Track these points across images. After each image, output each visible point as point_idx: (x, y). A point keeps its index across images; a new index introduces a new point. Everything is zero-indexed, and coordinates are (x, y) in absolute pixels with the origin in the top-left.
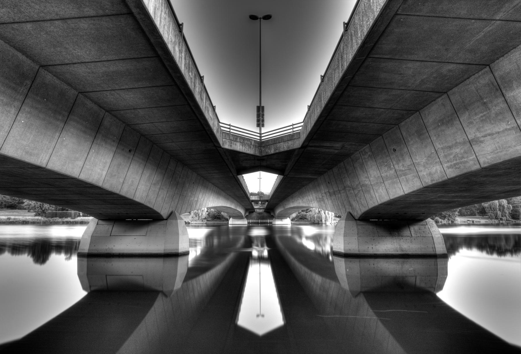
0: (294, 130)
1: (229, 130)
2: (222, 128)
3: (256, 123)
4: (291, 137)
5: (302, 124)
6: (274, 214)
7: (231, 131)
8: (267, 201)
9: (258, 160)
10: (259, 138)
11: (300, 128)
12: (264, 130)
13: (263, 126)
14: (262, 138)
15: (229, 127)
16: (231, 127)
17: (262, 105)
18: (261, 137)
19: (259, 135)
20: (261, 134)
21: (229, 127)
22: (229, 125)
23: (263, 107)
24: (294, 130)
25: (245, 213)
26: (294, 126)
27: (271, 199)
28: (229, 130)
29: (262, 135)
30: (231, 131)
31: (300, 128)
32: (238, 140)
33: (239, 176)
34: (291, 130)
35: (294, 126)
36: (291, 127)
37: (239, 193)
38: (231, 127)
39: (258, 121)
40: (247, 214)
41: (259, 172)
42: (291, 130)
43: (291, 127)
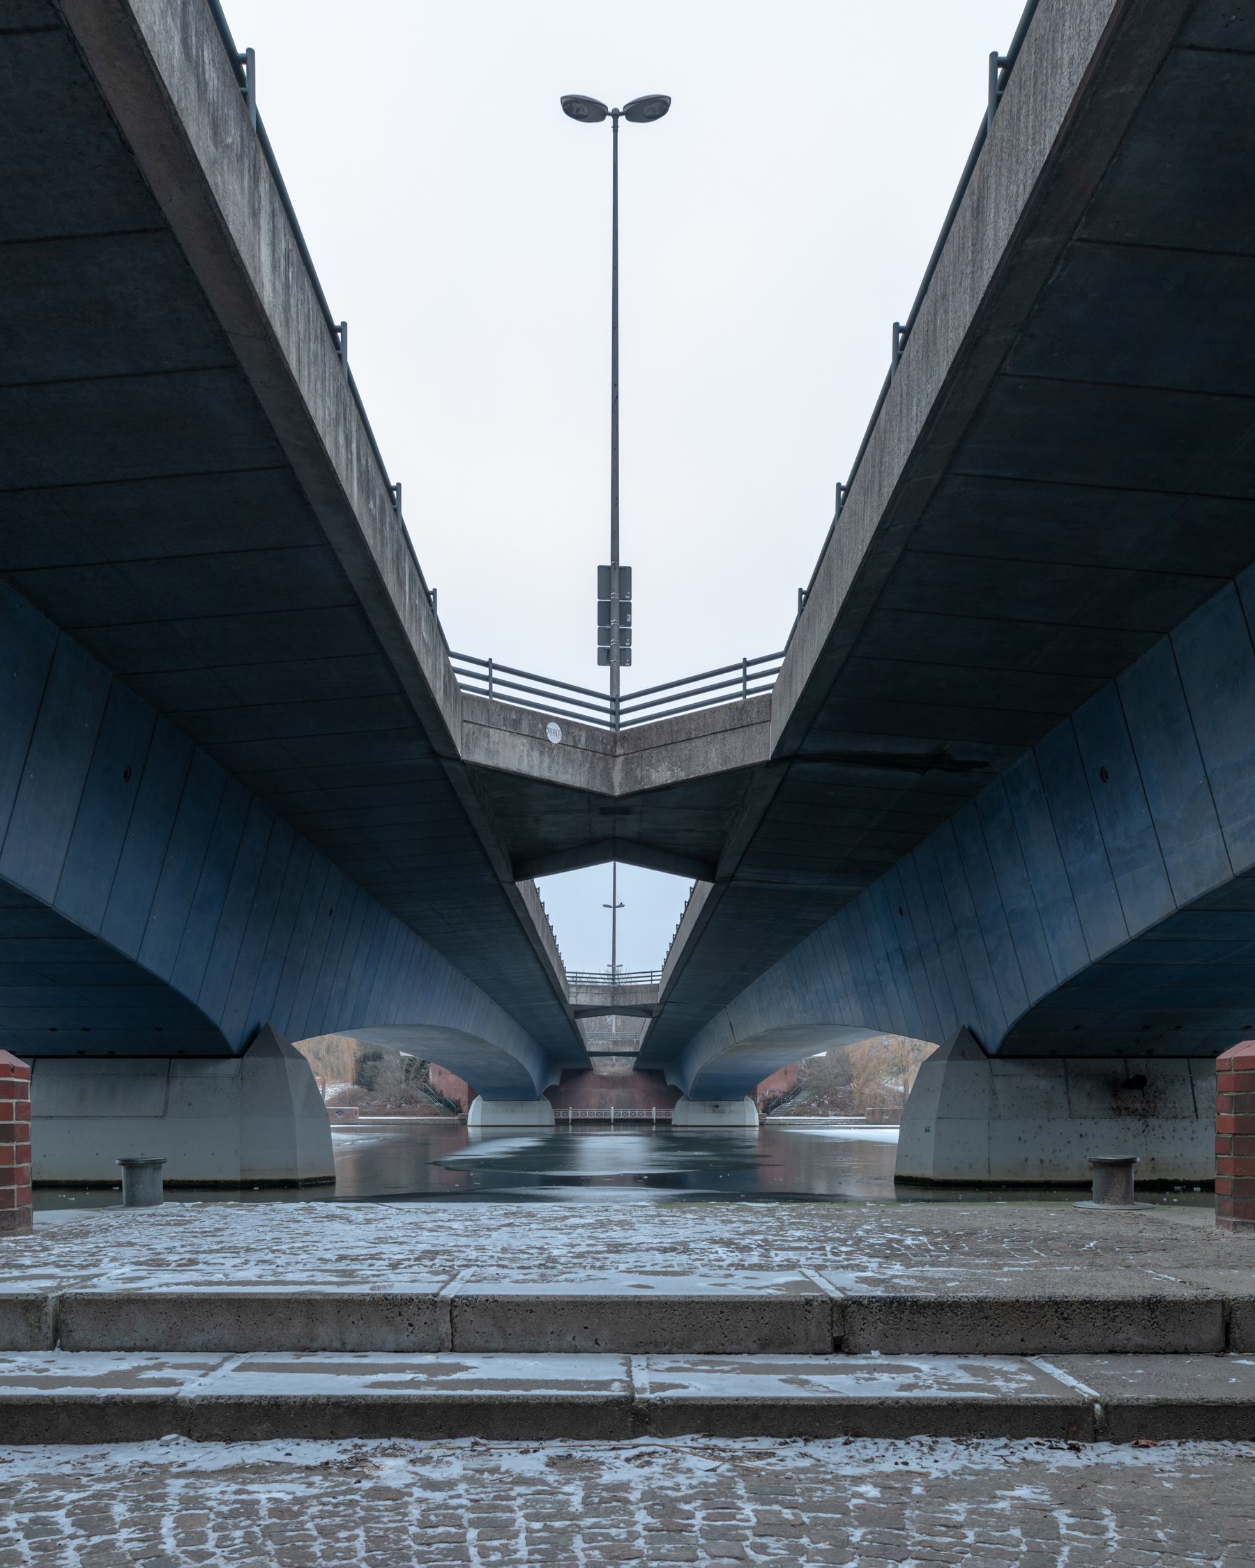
0: (751, 685)
1: (484, 685)
2: (461, 679)
3: (594, 646)
4: (742, 716)
5: (779, 663)
6: (682, 1077)
7: (497, 689)
8: (644, 1011)
9: (604, 812)
10: (606, 717)
11: (772, 679)
12: (631, 679)
13: (625, 658)
14: (624, 718)
15: (484, 671)
16: (497, 674)
17: (622, 563)
18: (615, 713)
19: (606, 704)
20: (615, 699)
21: (484, 671)
22: (488, 664)
23: (627, 571)
24: (751, 685)
25: (545, 1075)
26: (751, 670)
27: (664, 1001)
28: (484, 685)
30: (497, 689)
31: (772, 679)
32: (525, 727)
34: (738, 688)
35: (751, 670)
36: (738, 674)
38: (497, 674)
39: (604, 636)
40: (555, 1081)
42: (738, 688)
43: (738, 674)
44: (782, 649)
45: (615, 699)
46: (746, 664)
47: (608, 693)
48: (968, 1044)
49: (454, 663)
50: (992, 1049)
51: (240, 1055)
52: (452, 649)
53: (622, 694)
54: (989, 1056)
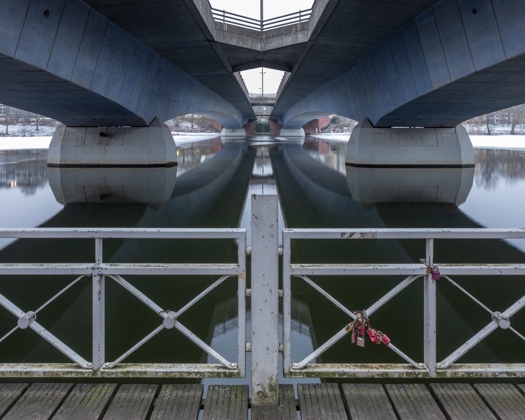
0: (302, 18)
1: (222, 18)
2: (214, 16)
5: (310, 12)
7: (226, 19)
8: (272, 105)
10: (259, 27)
14: (265, 27)
15: (222, 14)
16: (226, 14)
18: (262, 26)
19: (259, 23)
20: (262, 21)
21: (222, 14)
22: (223, 12)
24: (302, 18)
25: (243, 122)
26: (302, 14)
28: (222, 18)
29: (264, 23)
30: (226, 19)
31: (308, 16)
33: (236, 74)
34: (298, 19)
35: (302, 14)
36: (298, 15)
37: (235, 94)
38: (226, 14)
40: (246, 123)
41: (260, 69)
42: (298, 19)
43: (298, 15)
44: (311, 8)
45: (262, 21)
46: (301, 12)
47: (260, 20)
48: (367, 123)
49: (213, 11)
50: (375, 126)
51: (149, 126)
52: (213, 7)
53: (264, 20)
54: (374, 127)
